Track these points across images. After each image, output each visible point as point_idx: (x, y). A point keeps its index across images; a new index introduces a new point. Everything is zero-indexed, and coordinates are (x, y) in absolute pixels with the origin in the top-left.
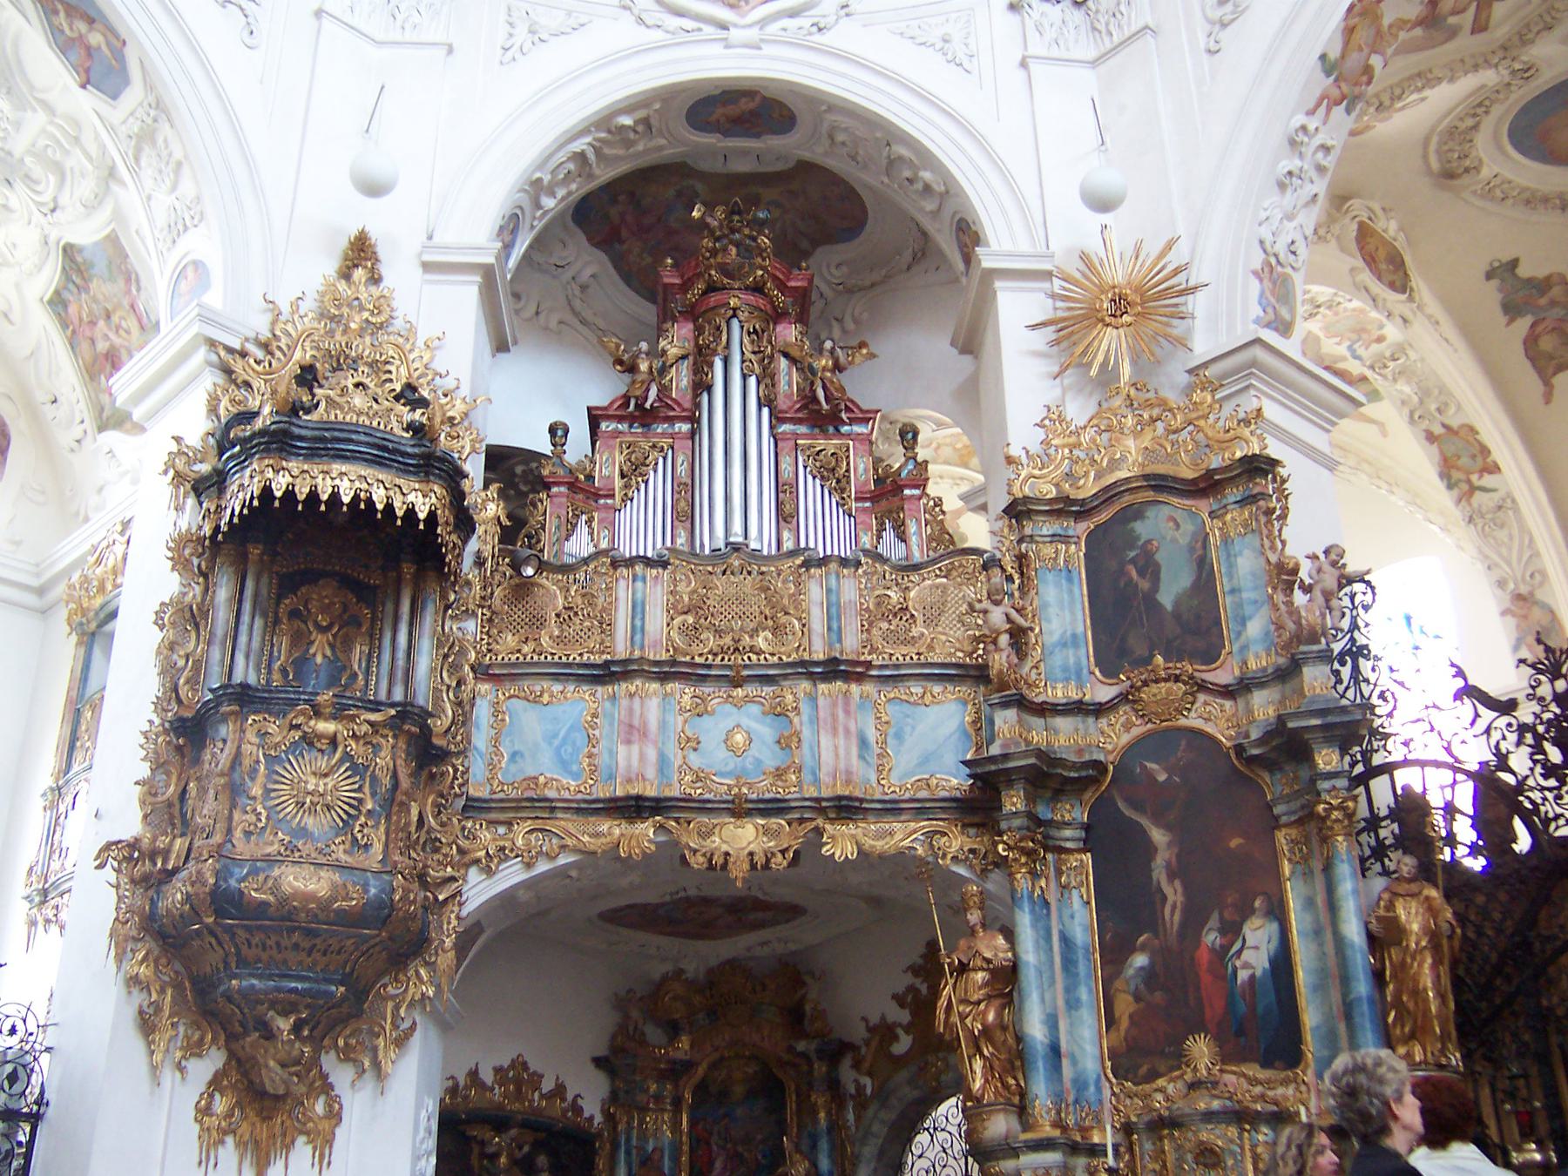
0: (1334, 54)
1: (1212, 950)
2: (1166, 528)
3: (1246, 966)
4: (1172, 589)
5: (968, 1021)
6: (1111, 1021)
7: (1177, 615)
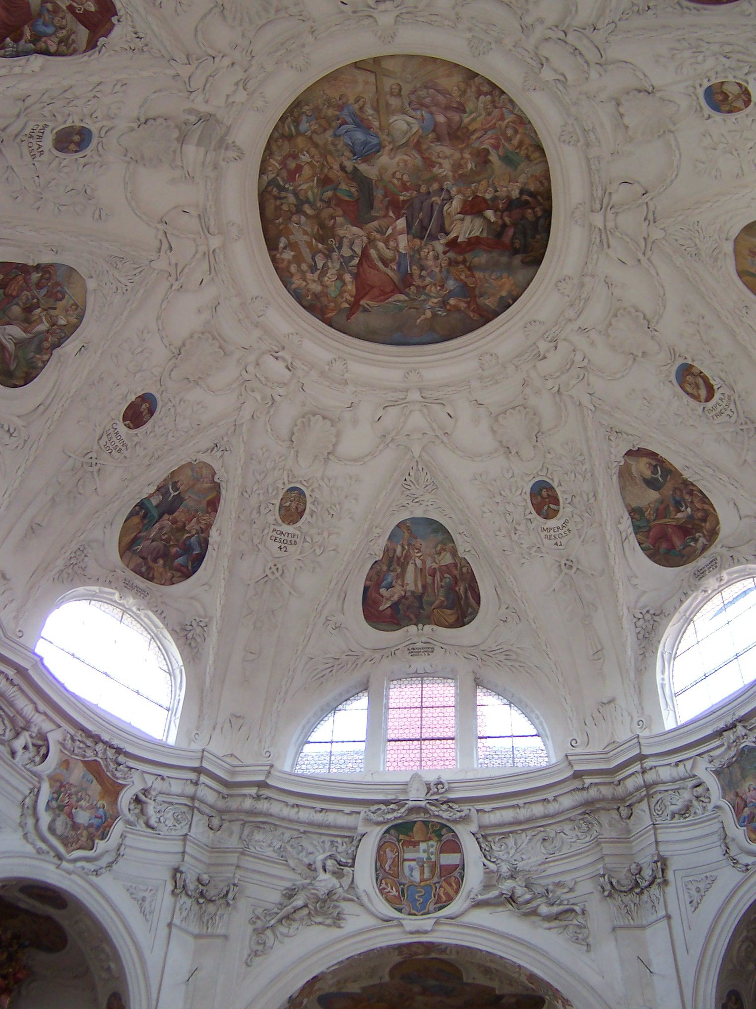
0: (294, 996)
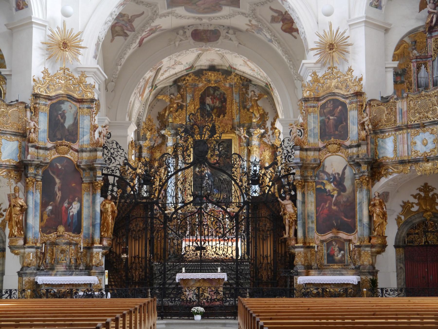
1: (66, 207)
2: (68, 108)
3: (72, 212)
4: (68, 123)
5: (15, 218)
6: (42, 220)
7: (68, 130)
